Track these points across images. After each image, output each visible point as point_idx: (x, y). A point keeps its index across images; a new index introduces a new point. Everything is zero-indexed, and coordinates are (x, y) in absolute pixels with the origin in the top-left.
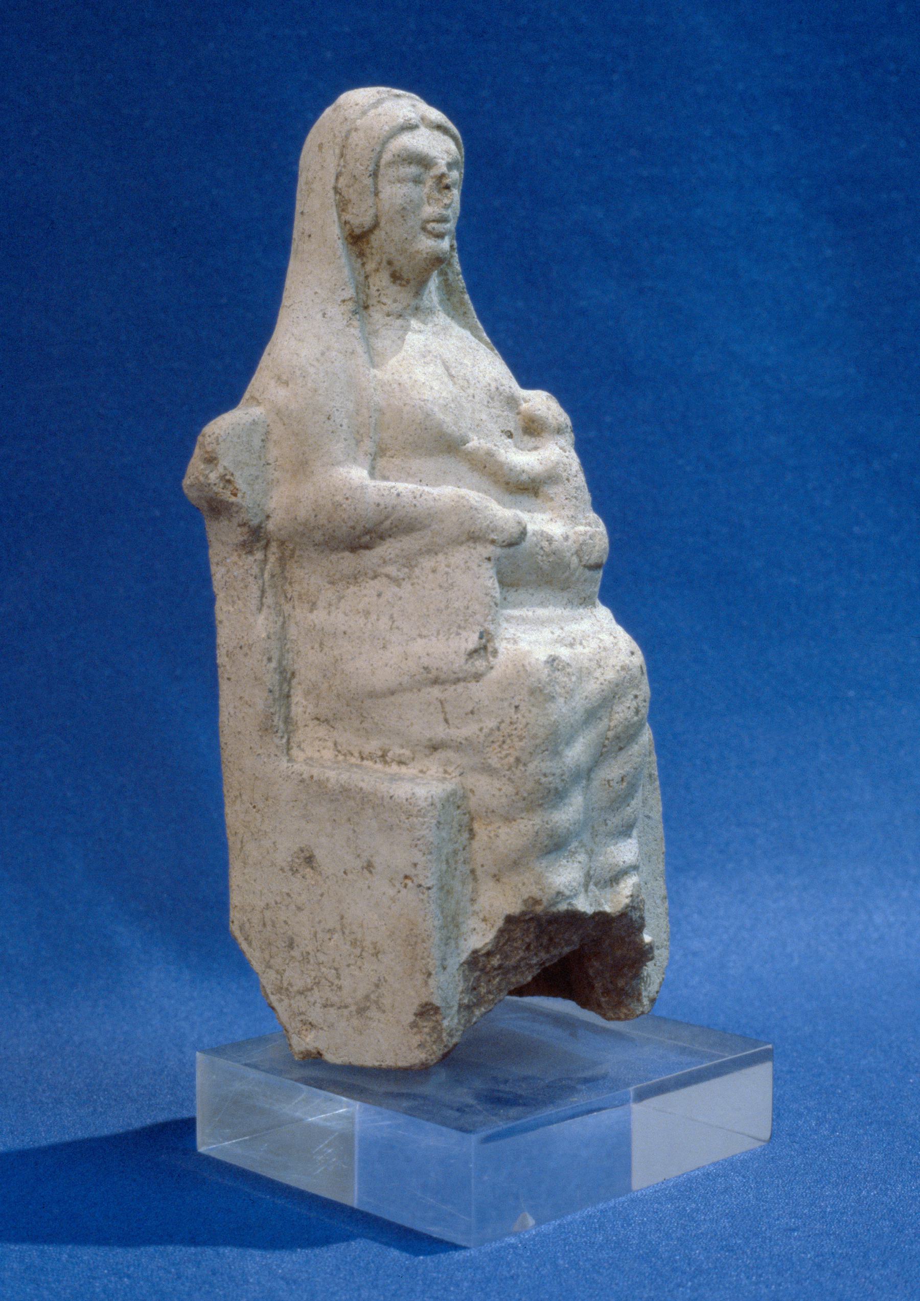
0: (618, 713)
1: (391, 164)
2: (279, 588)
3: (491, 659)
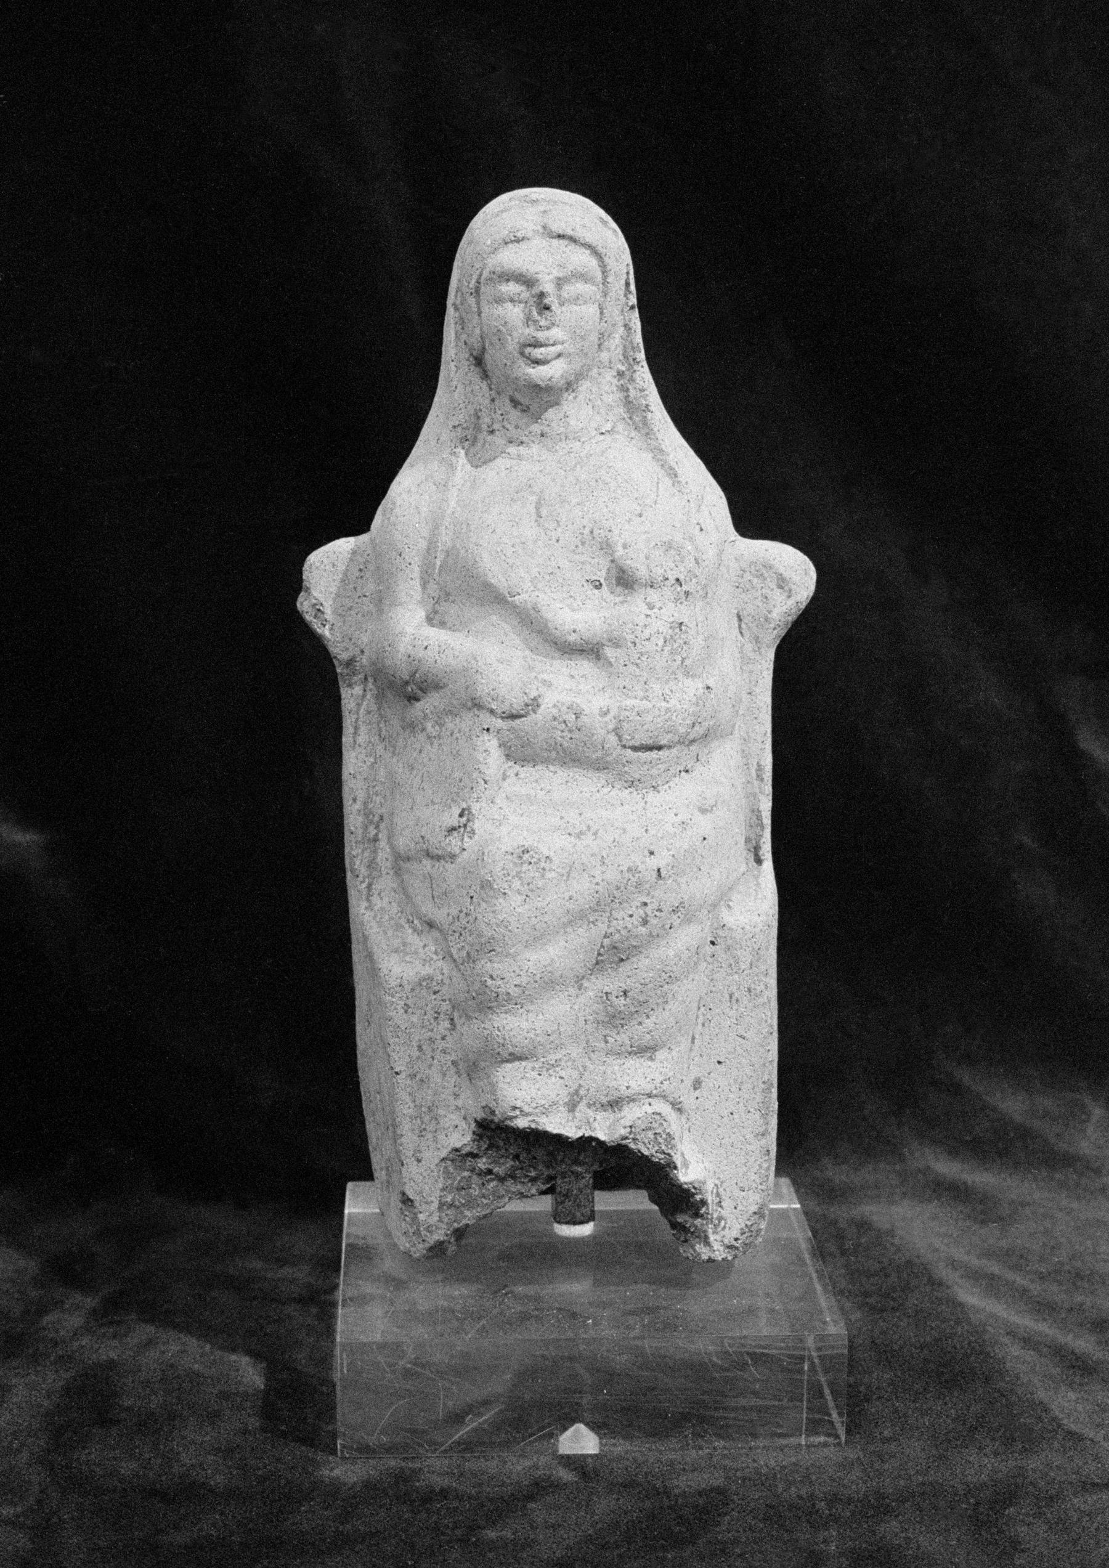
0: (617, 919)
1: (490, 280)
2: (375, 725)
3: (466, 839)
